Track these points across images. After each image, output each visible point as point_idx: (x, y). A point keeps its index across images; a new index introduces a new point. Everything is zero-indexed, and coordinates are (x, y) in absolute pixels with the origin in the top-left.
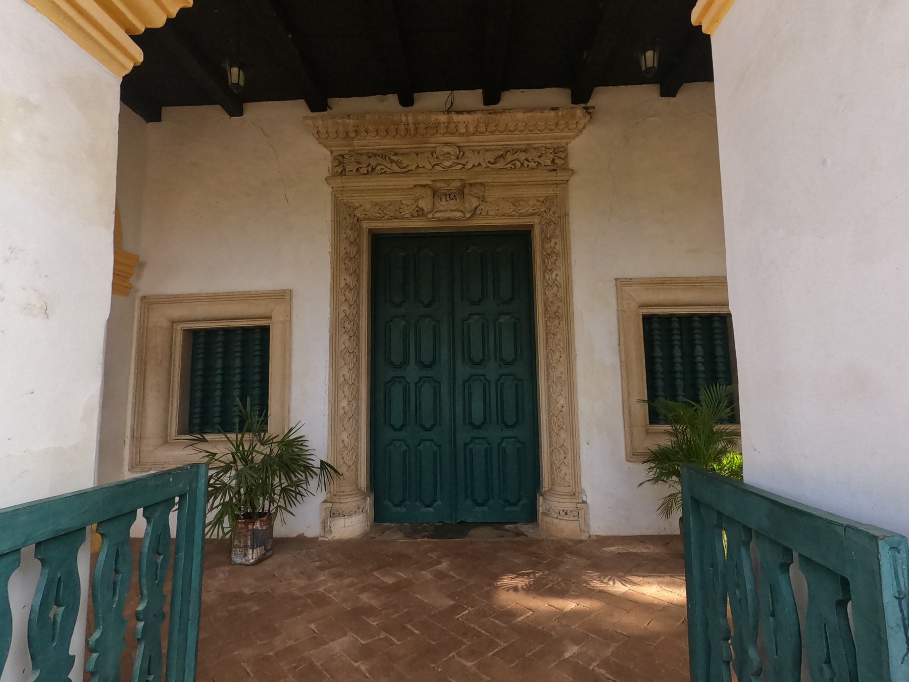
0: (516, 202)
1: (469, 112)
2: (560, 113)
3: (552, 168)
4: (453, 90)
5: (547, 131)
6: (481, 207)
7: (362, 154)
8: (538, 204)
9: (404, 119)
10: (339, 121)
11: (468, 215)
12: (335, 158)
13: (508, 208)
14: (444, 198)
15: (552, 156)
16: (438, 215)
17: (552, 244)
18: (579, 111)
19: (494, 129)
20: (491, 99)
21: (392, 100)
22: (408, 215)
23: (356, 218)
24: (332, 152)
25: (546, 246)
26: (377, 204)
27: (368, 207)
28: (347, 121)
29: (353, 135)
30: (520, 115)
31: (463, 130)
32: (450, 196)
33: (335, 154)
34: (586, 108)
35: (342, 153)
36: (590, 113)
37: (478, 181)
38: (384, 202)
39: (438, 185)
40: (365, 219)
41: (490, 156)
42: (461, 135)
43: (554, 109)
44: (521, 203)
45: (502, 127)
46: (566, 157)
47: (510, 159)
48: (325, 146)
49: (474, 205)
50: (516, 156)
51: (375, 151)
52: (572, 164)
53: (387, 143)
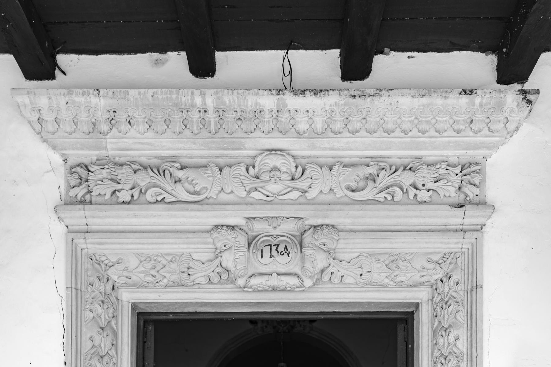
0: (393, 261)
1: (316, 92)
2: (478, 100)
3: (455, 200)
4: (288, 46)
5: (450, 132)
6: (331, 269)
7: (122, 165)
8: (430, 266)
9: (198, 101)
10: (81, 99)
11: (308, 283)
12: (71, 171)
13: (380, 274)
14: (266, 250)
15: (457, 180)
16: (254, 282)
17: (451, 338)
18: (511, 94)
19: (358, 125)
20: (355, 68)
21: (177, 61)
22: (203, 280)
23: (110, 284)
24: (65, 161)
25: (441, 341)
26: (148, 259)
27: (133, 262)
28: (94, 100)
29: (104, 127)
30: (406, 101)
31: (302, 127)
32: (278, 248)
33: (71, 162)
34: (524, 93)
35: (86, 161)
36: (530, 102)
37: (327, 221)
38: (162, 255)
39: (259, 227)
40: (128, 285)
41: (351, 177)
42: (300, 134)
43: (468, 92)
44: (401, 264)
45: (373, 120)
46: (483, 180)
47: (382, 186)
48: (54, 148)
49: (320, 265)
50: (394, 178)
51: (144, 160)
52: (493, 192)
53: (166, 146)
